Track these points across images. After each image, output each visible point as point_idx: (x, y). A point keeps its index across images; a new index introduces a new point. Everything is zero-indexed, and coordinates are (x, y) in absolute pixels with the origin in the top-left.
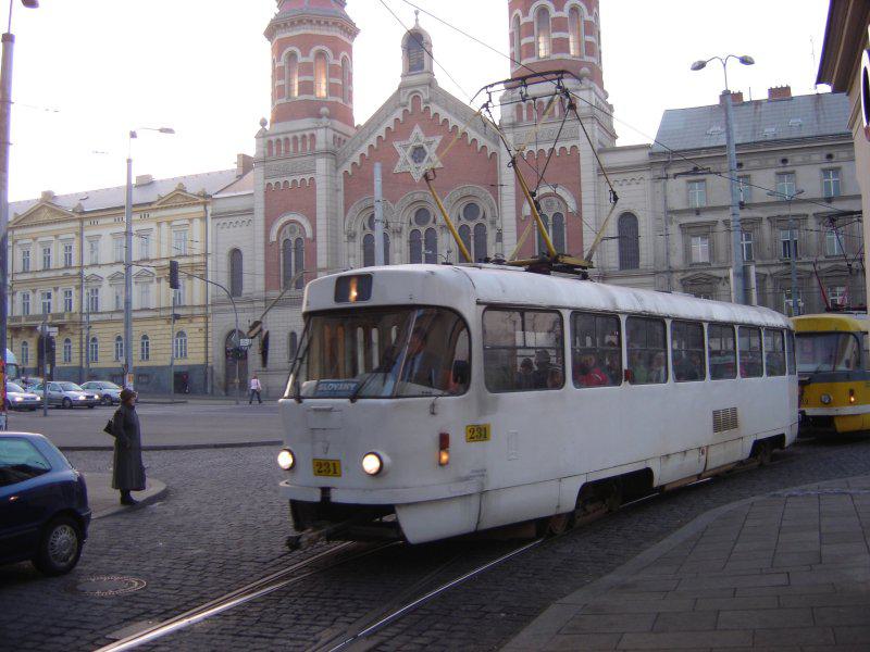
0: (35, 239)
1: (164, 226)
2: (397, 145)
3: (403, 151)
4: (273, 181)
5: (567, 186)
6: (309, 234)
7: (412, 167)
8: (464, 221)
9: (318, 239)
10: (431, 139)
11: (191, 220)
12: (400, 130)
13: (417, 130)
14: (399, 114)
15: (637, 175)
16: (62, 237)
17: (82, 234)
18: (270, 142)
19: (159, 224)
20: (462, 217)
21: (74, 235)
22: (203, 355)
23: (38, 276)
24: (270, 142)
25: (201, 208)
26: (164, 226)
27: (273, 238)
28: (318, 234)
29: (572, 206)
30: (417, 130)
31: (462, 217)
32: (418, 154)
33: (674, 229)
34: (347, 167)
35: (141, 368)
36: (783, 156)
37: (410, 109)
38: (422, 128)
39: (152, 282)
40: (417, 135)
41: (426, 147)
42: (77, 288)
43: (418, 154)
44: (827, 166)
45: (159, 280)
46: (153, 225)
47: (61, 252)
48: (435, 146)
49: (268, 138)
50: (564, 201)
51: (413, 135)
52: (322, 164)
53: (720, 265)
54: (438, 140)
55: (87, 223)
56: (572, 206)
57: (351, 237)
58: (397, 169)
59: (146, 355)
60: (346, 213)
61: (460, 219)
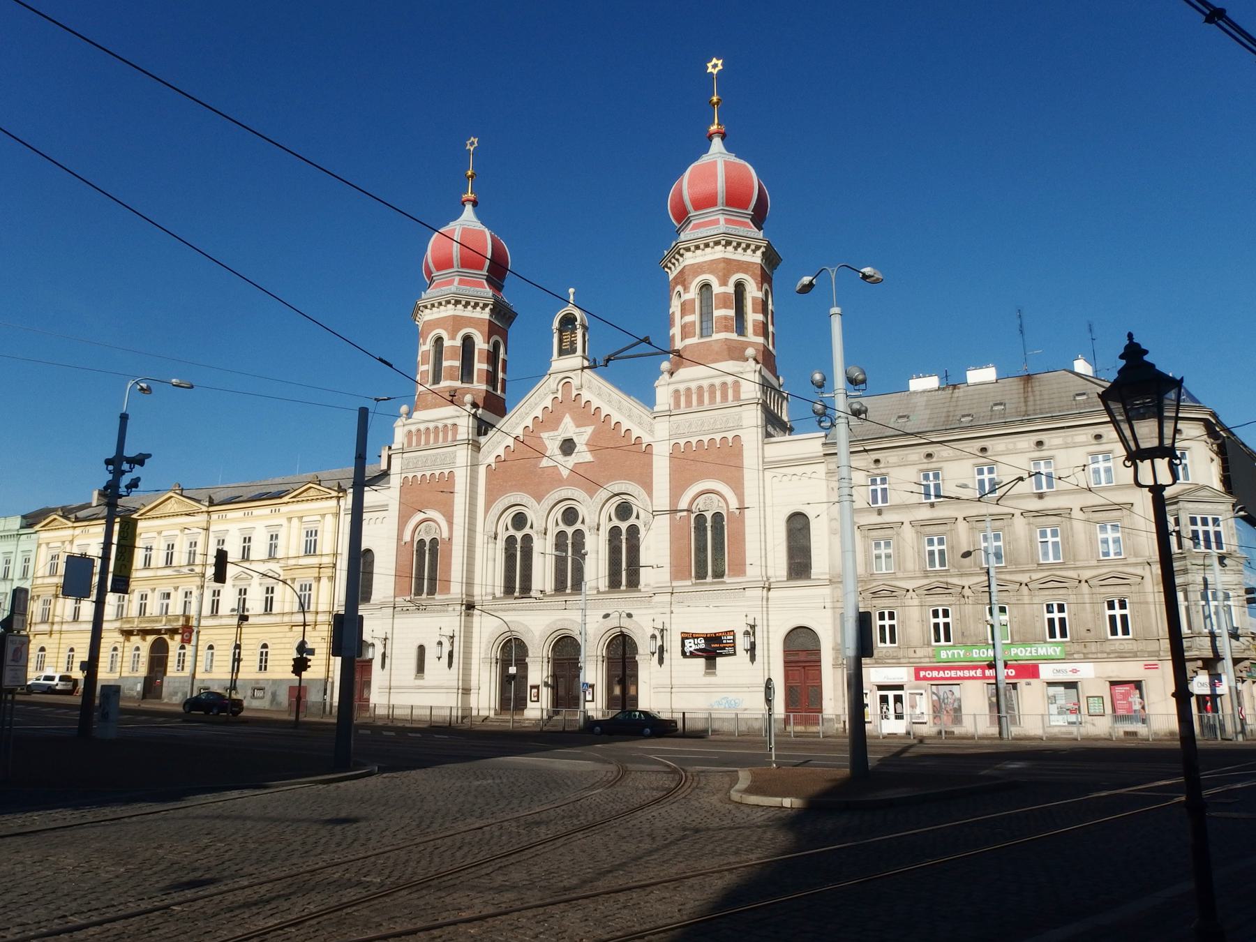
0: (160, 533)
1: (295, 521)
2: (544, 435)
3: (552, 444)
4: (410, 476)
5: (727, 482)
6: (445, 535)
8: (616, 522)
9: (455, 540)
10: (582, 429)
11: (323, 516)
12: (549, 420)
13: (567, 419)
14: (548, 402)
15: (808, 469)
17: (207, 529)
19: (290, 519)
20: (613, 517)
22: (323, 669)
23: (160, 573)
24: (410, 432)
25: (334, 502)
26: (295, 521)
27: (407, 537)
28: (455, 534)
30: (567, 419)
31: (613, 517)
32: (568, 447)
34: (491, 460)
35: (257, 681)
37: (559, 395)
38: (574, 419)
40: (568, 428)
43: (568, 447)
44: (1037, 454)
46: (284, 521)
47: (186, 548)
48: (586, 437)
49: (407, 428)
50: (725, 499)
51: (562, 425)
52: (462, 455)
53: (906, 575)
54: (589, 430)
55: (214, 516)
59: (263, 667)
60: (486, 512)
61: (610, 519)
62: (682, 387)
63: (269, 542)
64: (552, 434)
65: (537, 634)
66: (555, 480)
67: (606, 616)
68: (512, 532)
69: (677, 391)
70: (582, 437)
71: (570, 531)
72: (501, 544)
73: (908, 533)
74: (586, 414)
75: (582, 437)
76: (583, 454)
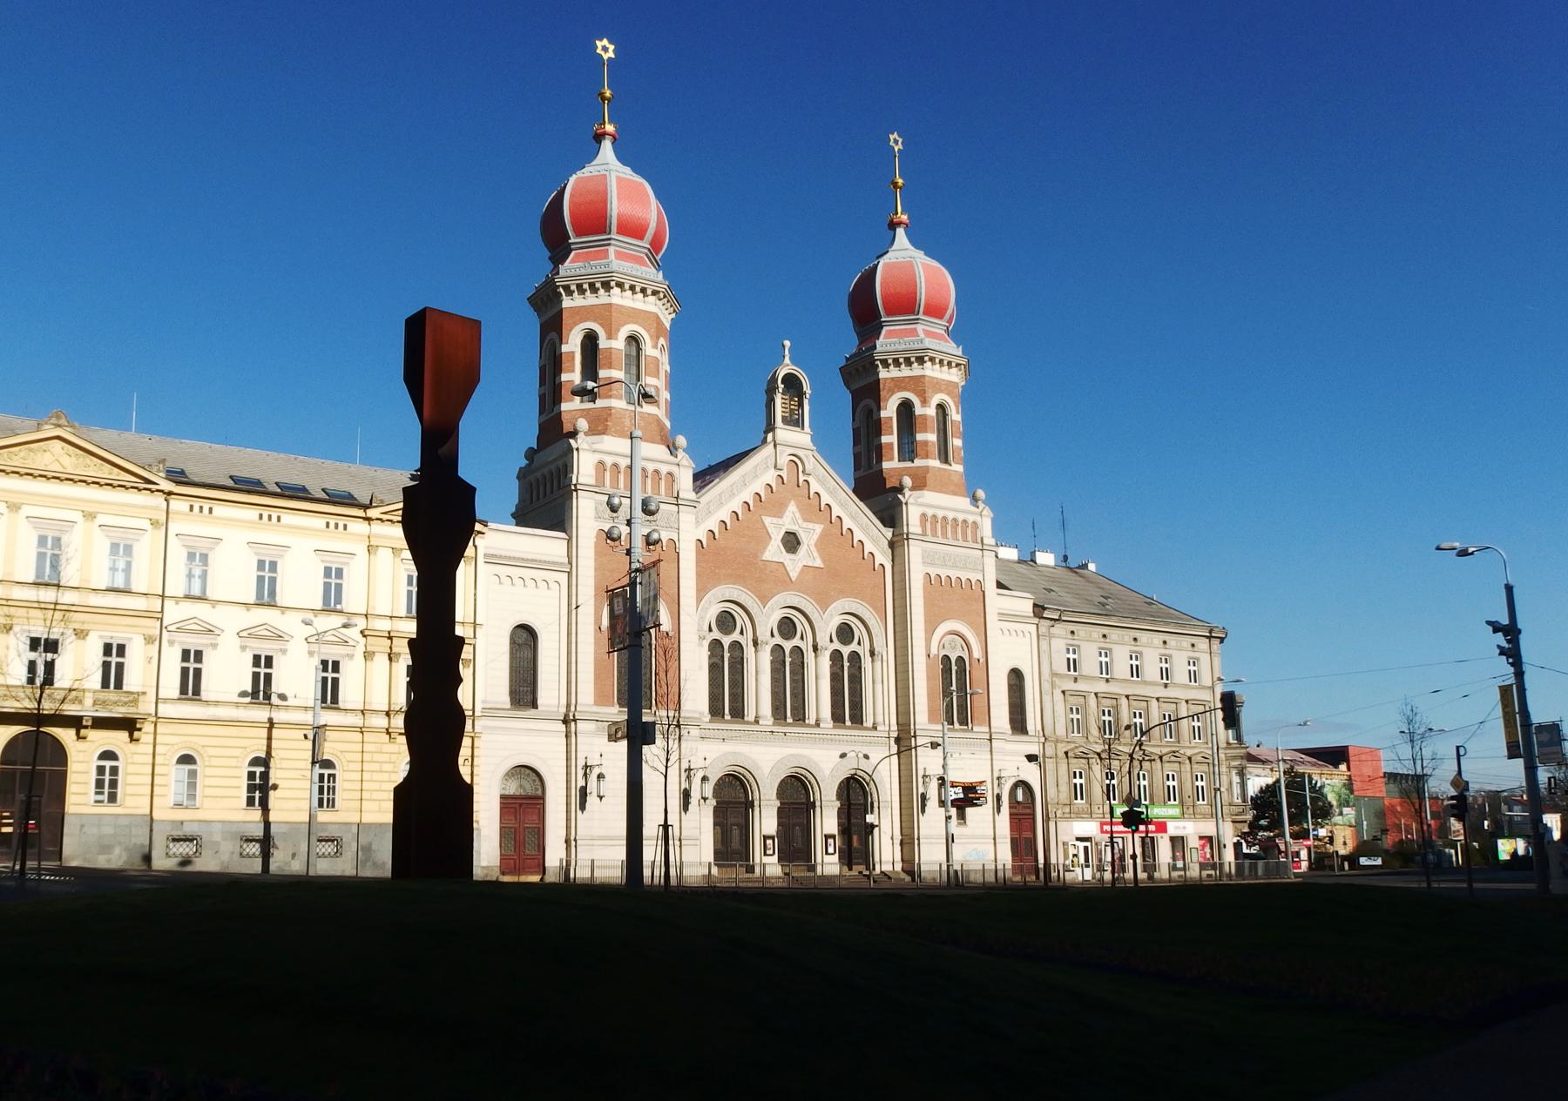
3: (775, 528)
7: (786, 558)
10: (810, 525)
16: (101, 519)
18: (601, 463)
21: (146, 524)
24: (601, 463)
29: (977, 653)
32: (792, 542)
33: (1058, 693)
36: (1105, 630)
39: (351, 657)
40: (791, 518)
41: (802, 536)
42: (149, 640)
43: (792, 542)
45: (368, 655)
46: (361, 550)
54: (819, 528)
56: (977, 653)
57: (702, 638)
58: (767, 556)
62: (930, 512)
63: (321, 580)
64: (775, 520)
65: (766, 771)
66: (777, 579)
67: (843, 756)
68: (716, 634)
69: (924, 515)
70: (810, 534)
71: (788, 645)
72: (706, 644)
73: (1092, 701)
74: (816, 509)
75: (810, 534)
76: (808, 555)
